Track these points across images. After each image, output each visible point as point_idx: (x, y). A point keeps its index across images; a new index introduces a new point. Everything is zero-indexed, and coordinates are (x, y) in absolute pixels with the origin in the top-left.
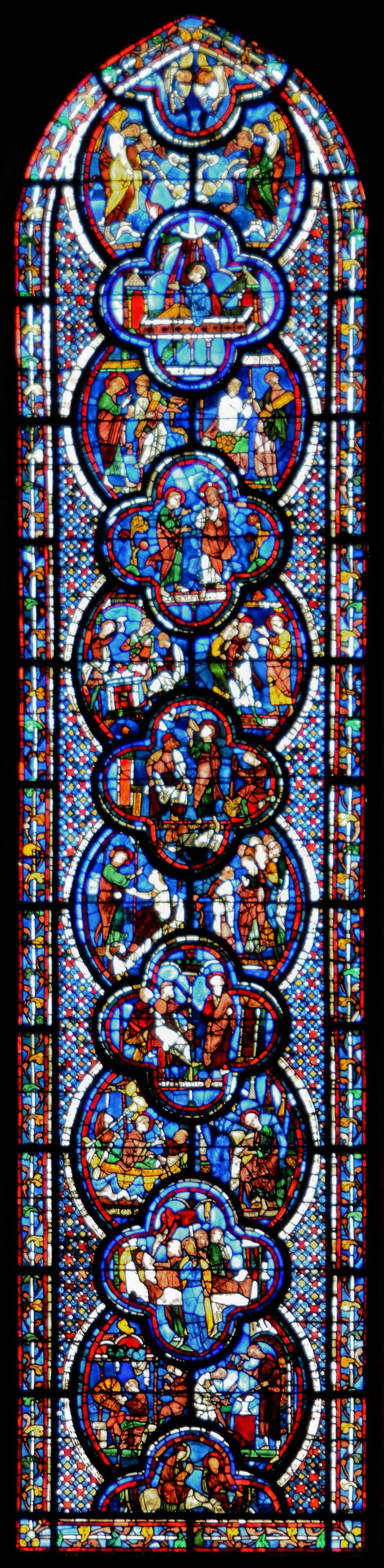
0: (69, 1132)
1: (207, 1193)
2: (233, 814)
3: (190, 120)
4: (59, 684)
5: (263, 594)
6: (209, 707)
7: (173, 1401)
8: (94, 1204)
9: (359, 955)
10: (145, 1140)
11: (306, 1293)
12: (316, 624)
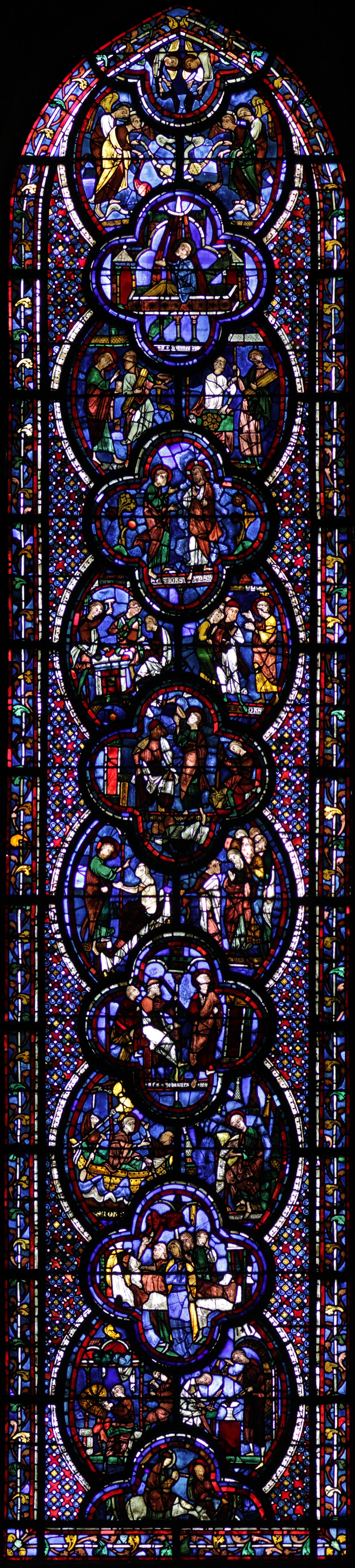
0: (55, 1132)
1: (192, 1195)
2: (220, 805)
3: (177, 103)
4: (48, 668)
5: (250, 577)
6: (196, 694)
7: (159, 1407)
8: (81, 1207)
9: (344, 953)
10: (131, 1142)
11: (289, 1297)
12: (302, 610)
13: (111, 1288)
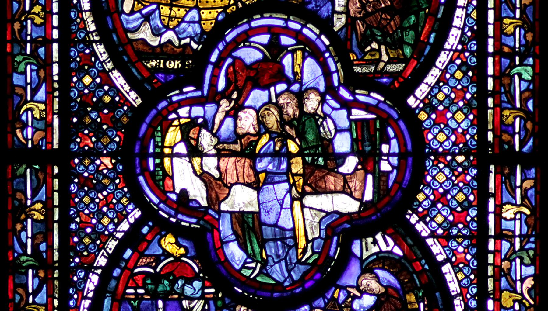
1: (297, 35)
8: (125, 53)
11: (447, 192)
13: (172, 178)
